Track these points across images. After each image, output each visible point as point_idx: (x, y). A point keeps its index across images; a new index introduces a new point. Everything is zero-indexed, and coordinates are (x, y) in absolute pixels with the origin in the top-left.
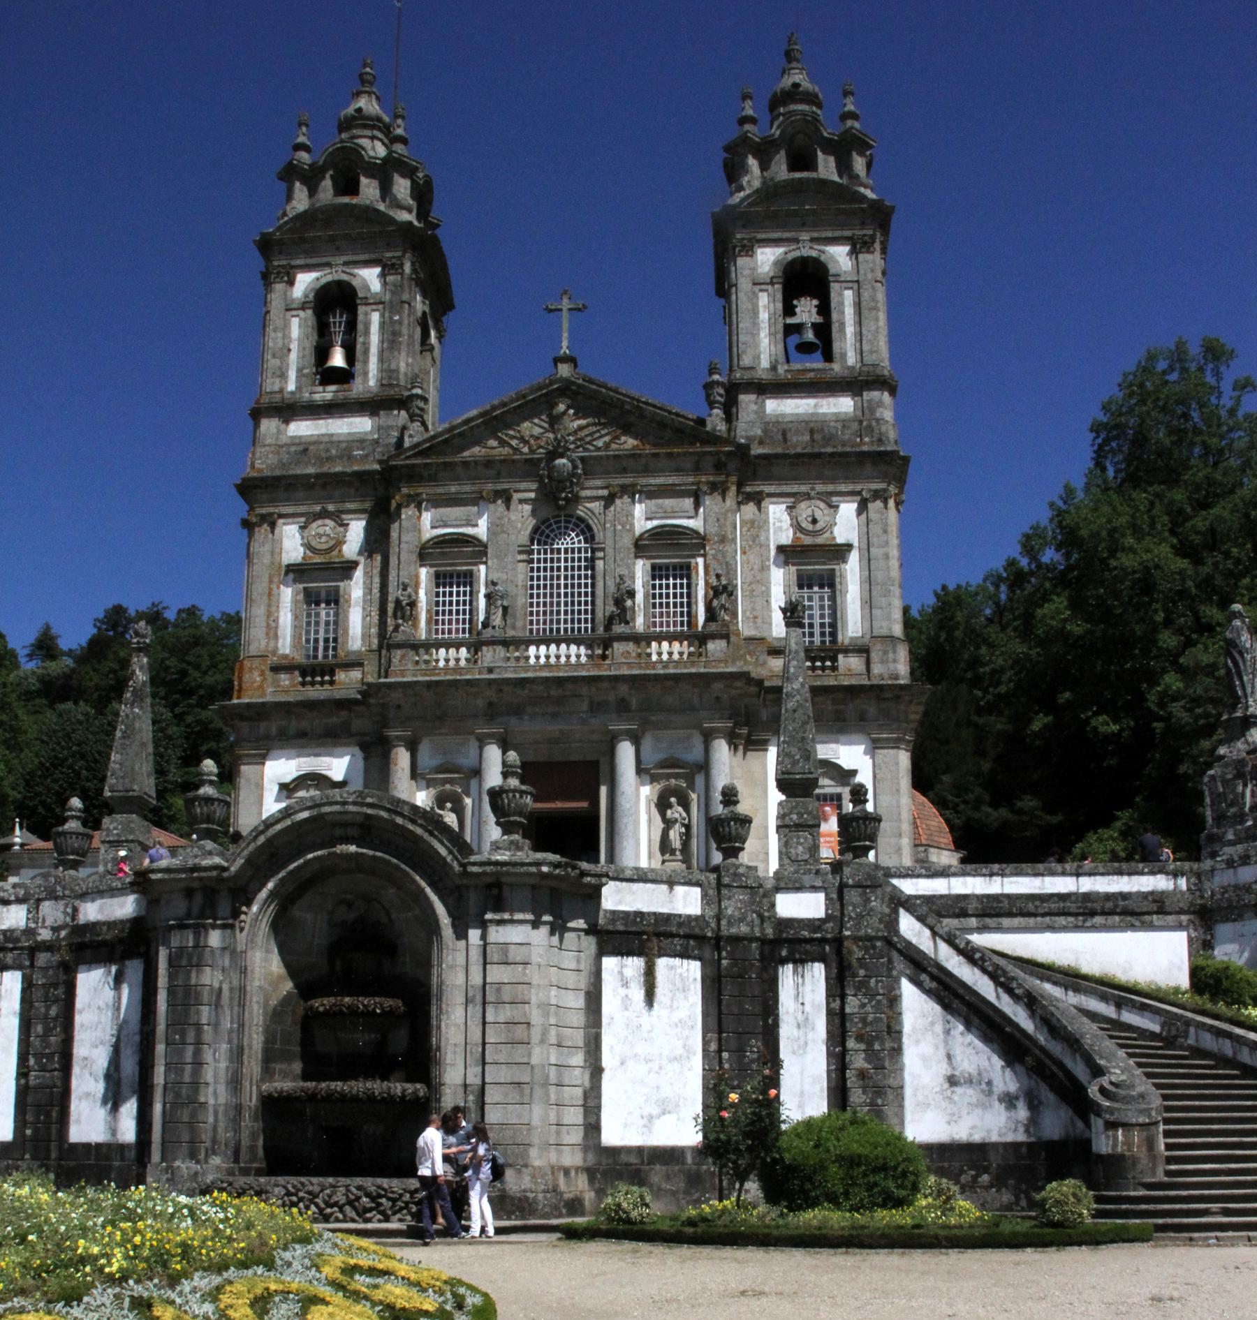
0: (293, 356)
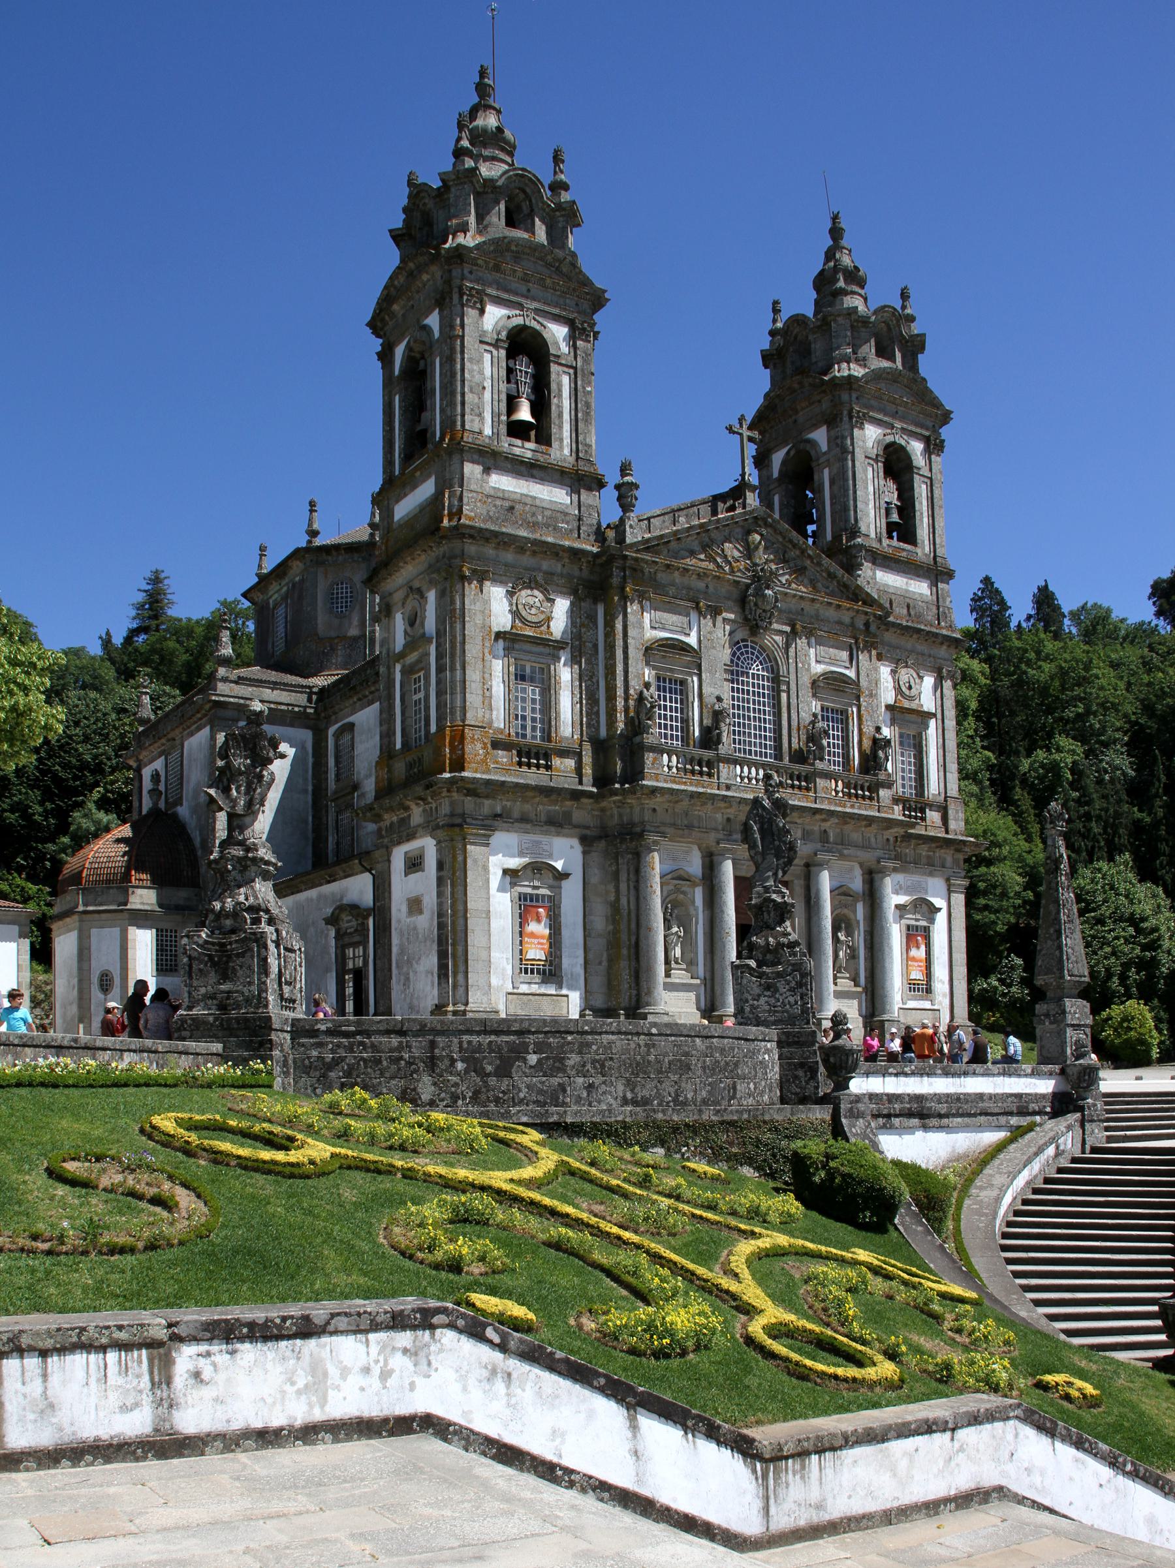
0: (487, 395)
